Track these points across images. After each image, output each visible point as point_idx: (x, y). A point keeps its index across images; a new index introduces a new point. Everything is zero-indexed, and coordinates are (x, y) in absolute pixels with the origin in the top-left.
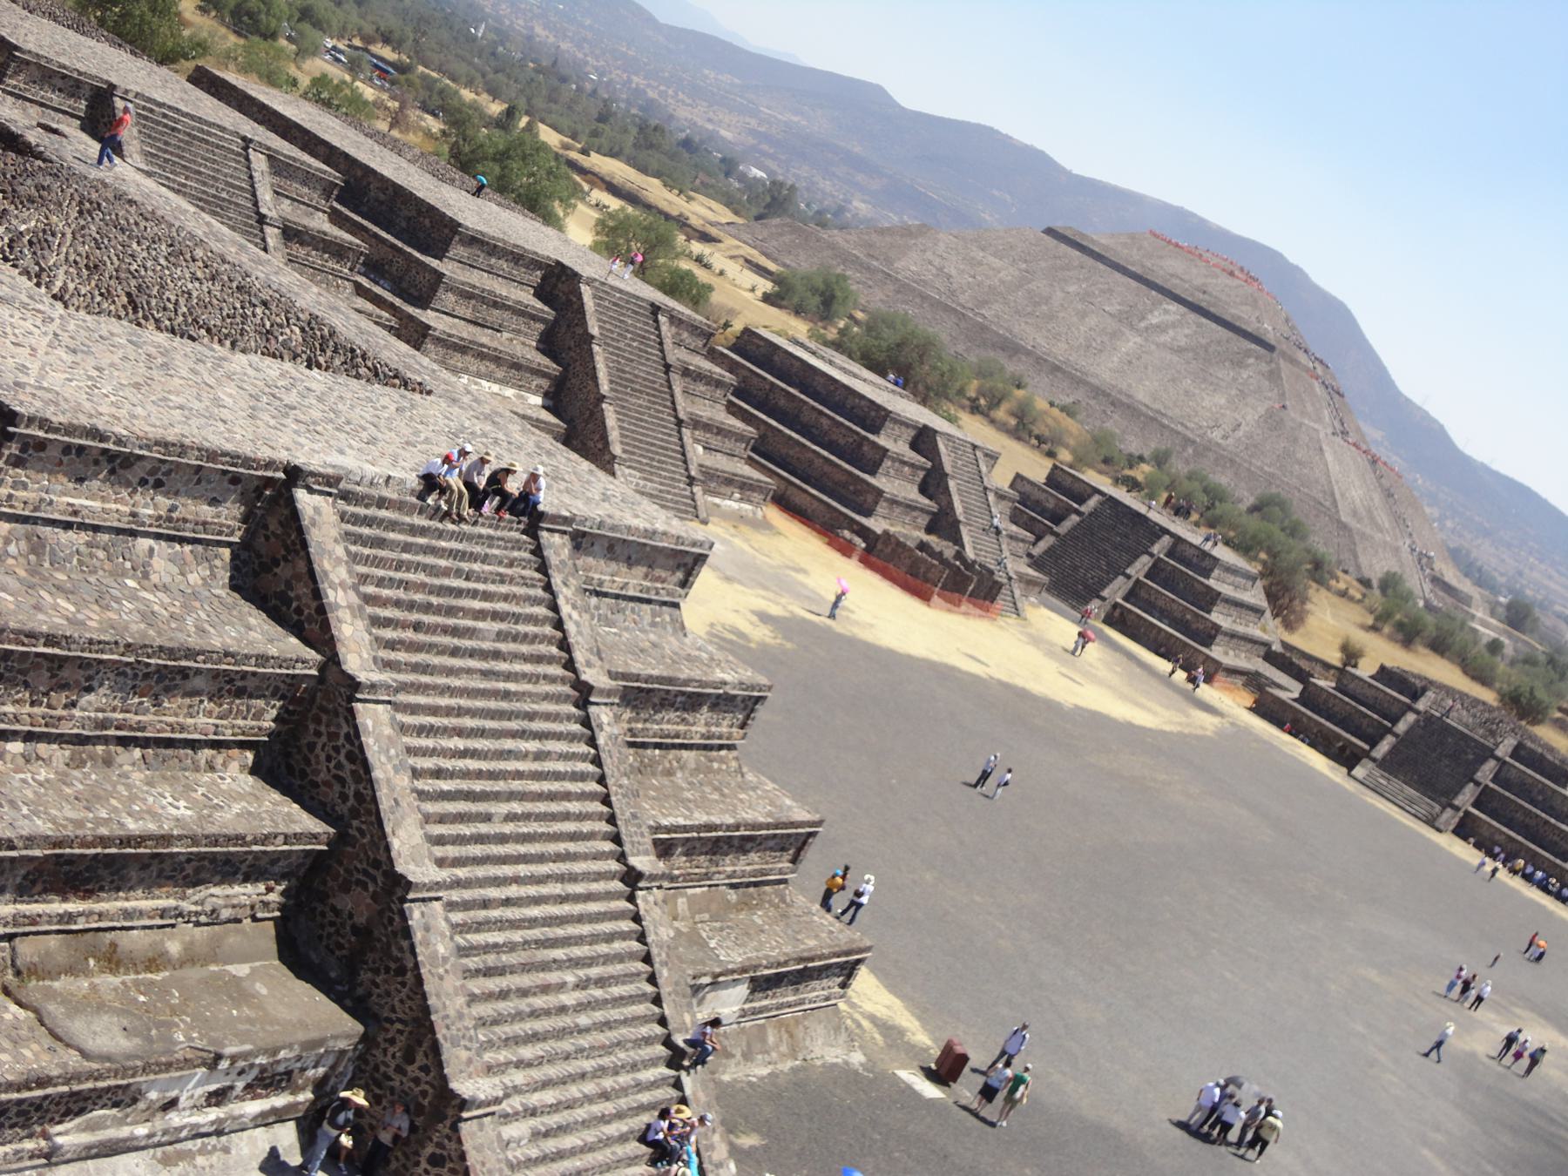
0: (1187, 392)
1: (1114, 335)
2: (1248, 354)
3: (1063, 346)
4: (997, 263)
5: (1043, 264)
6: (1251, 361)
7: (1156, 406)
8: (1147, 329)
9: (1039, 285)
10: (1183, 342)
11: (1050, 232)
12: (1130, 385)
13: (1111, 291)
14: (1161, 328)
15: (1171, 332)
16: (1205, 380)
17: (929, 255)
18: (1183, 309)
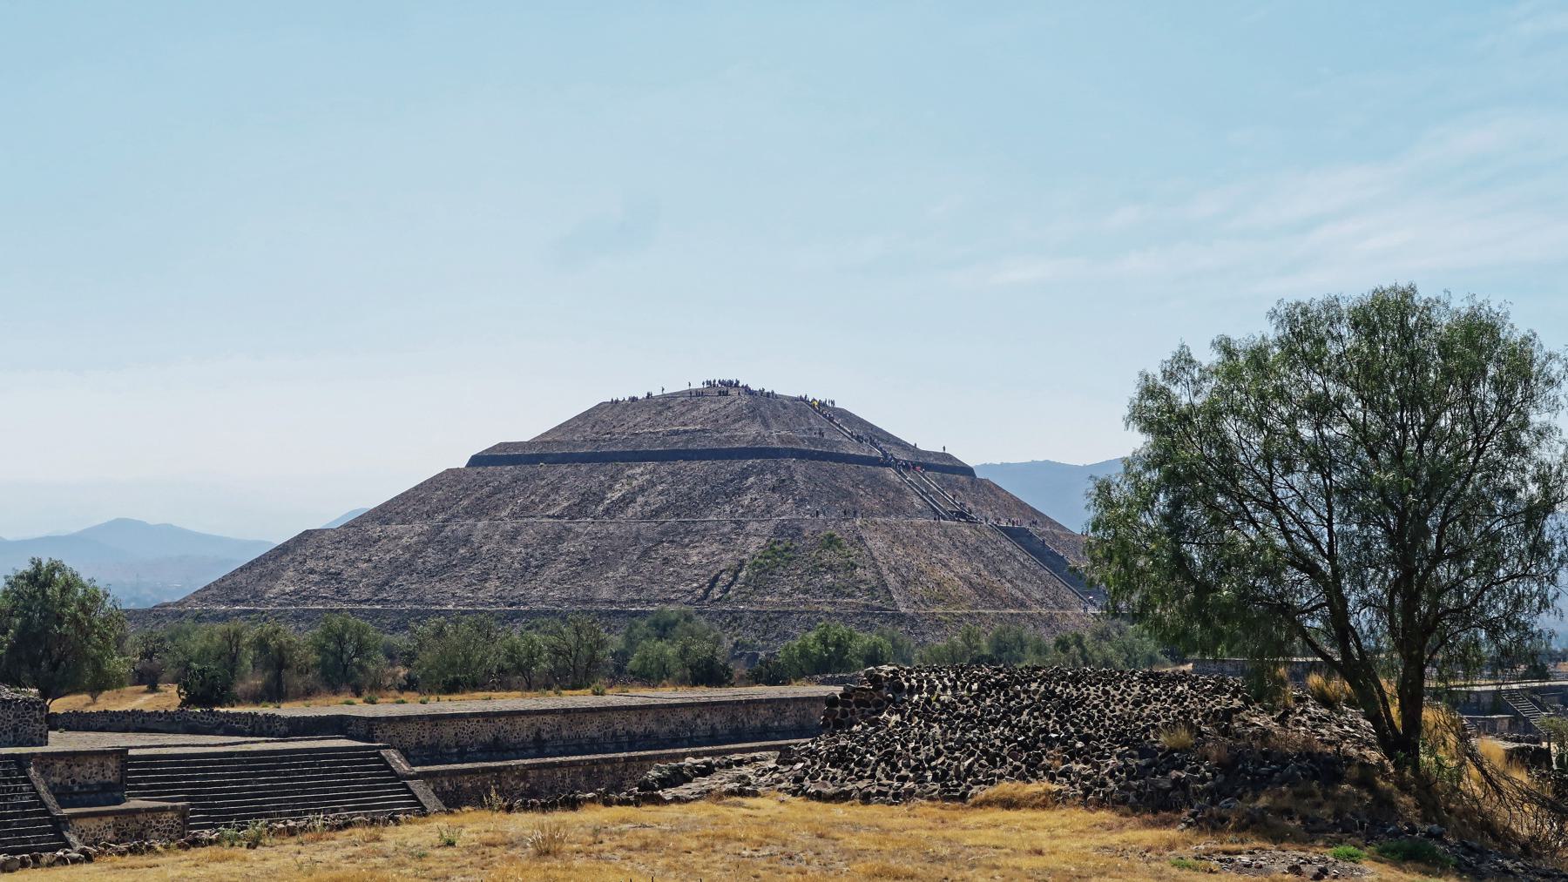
0: (666, 561)
1: (559, 538)
2: (745, 474)
3: (492, 585)
4: (394, 528)
5: (465, 503)
6: (752, 479)
7: (625, 597)
8: (607, 511)
9: (457, 528)
10: (656, 501)
11: (476, 461)
12: (588, 588)
13: (556, 490)
14: (627, 501)
15: (640, 499)
16: (688, 533)
17: (310, 564)
18: (651, 465)
